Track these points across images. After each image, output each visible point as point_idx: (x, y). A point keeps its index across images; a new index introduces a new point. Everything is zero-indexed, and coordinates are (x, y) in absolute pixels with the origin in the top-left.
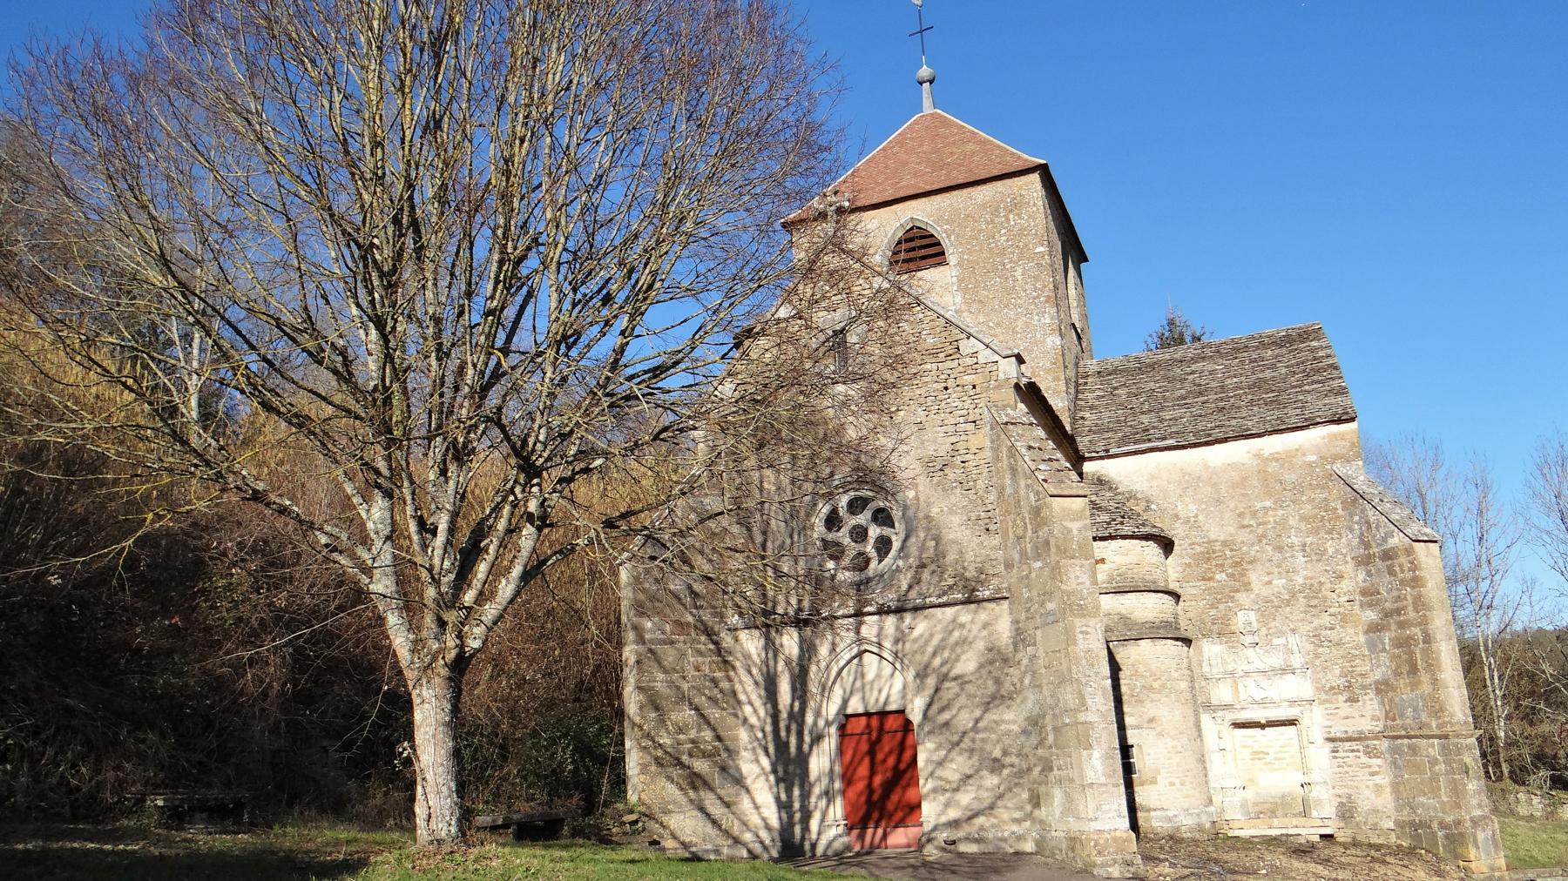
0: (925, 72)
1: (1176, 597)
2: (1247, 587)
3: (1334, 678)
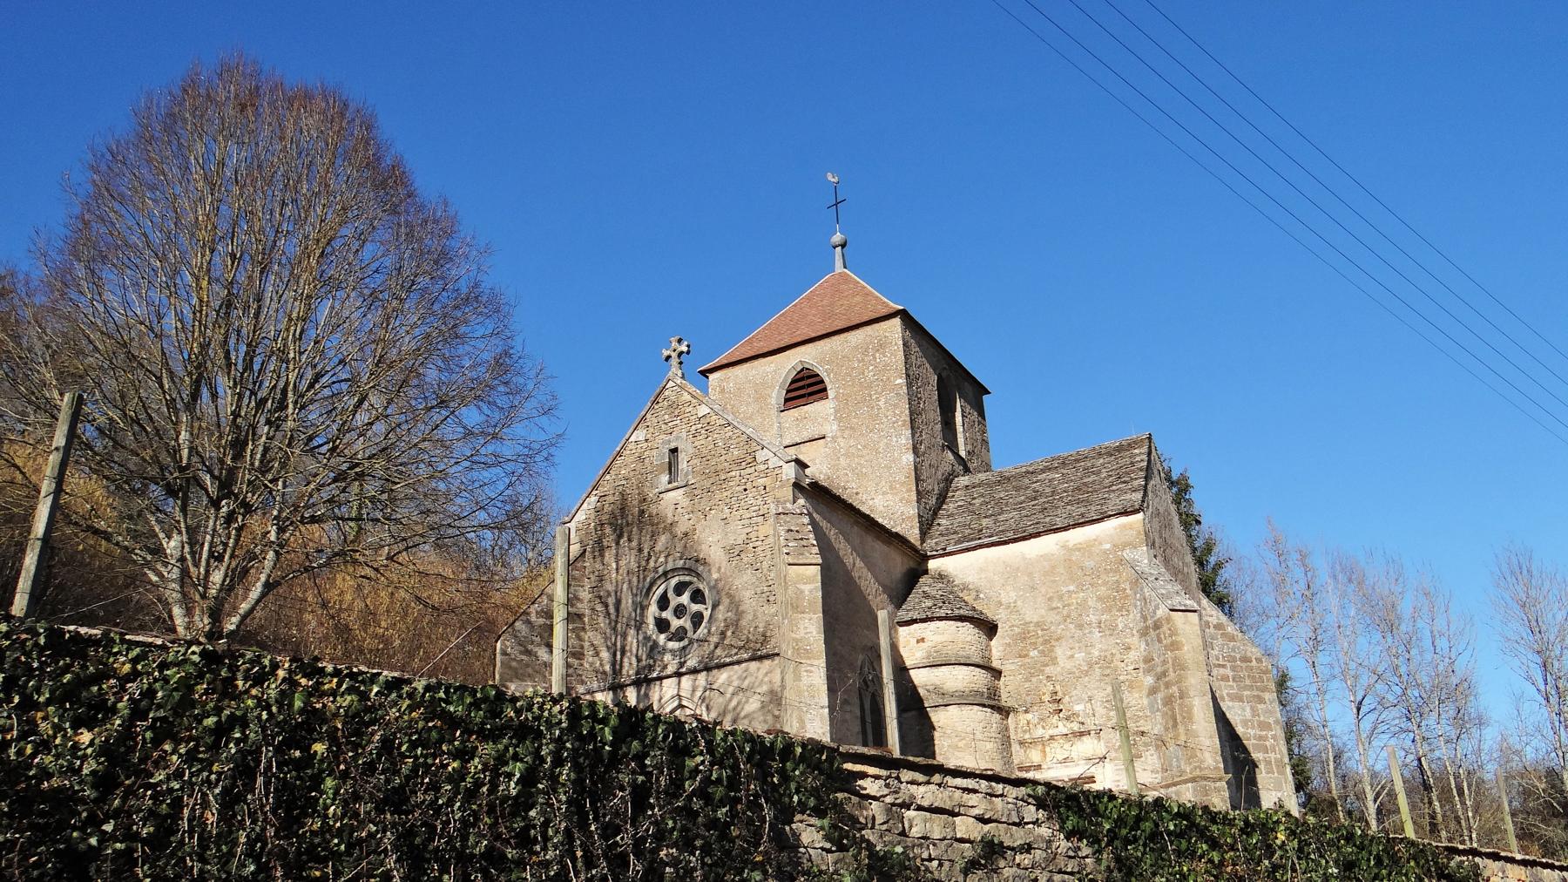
0: (837, 238)
1: (997, 674)
2: (1054, 661)
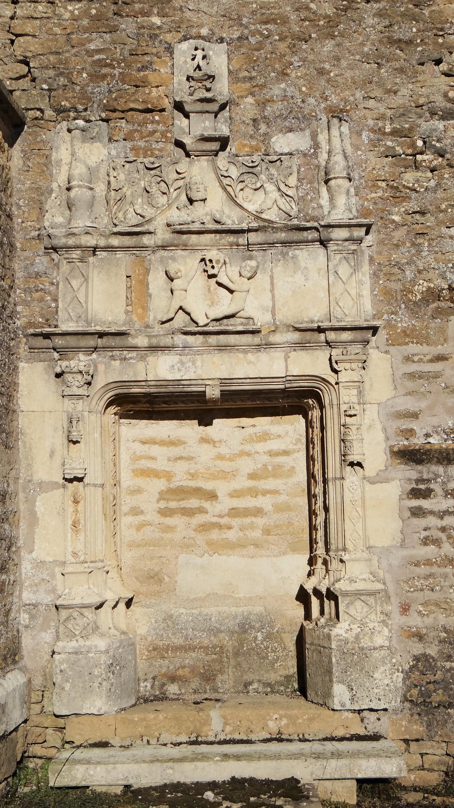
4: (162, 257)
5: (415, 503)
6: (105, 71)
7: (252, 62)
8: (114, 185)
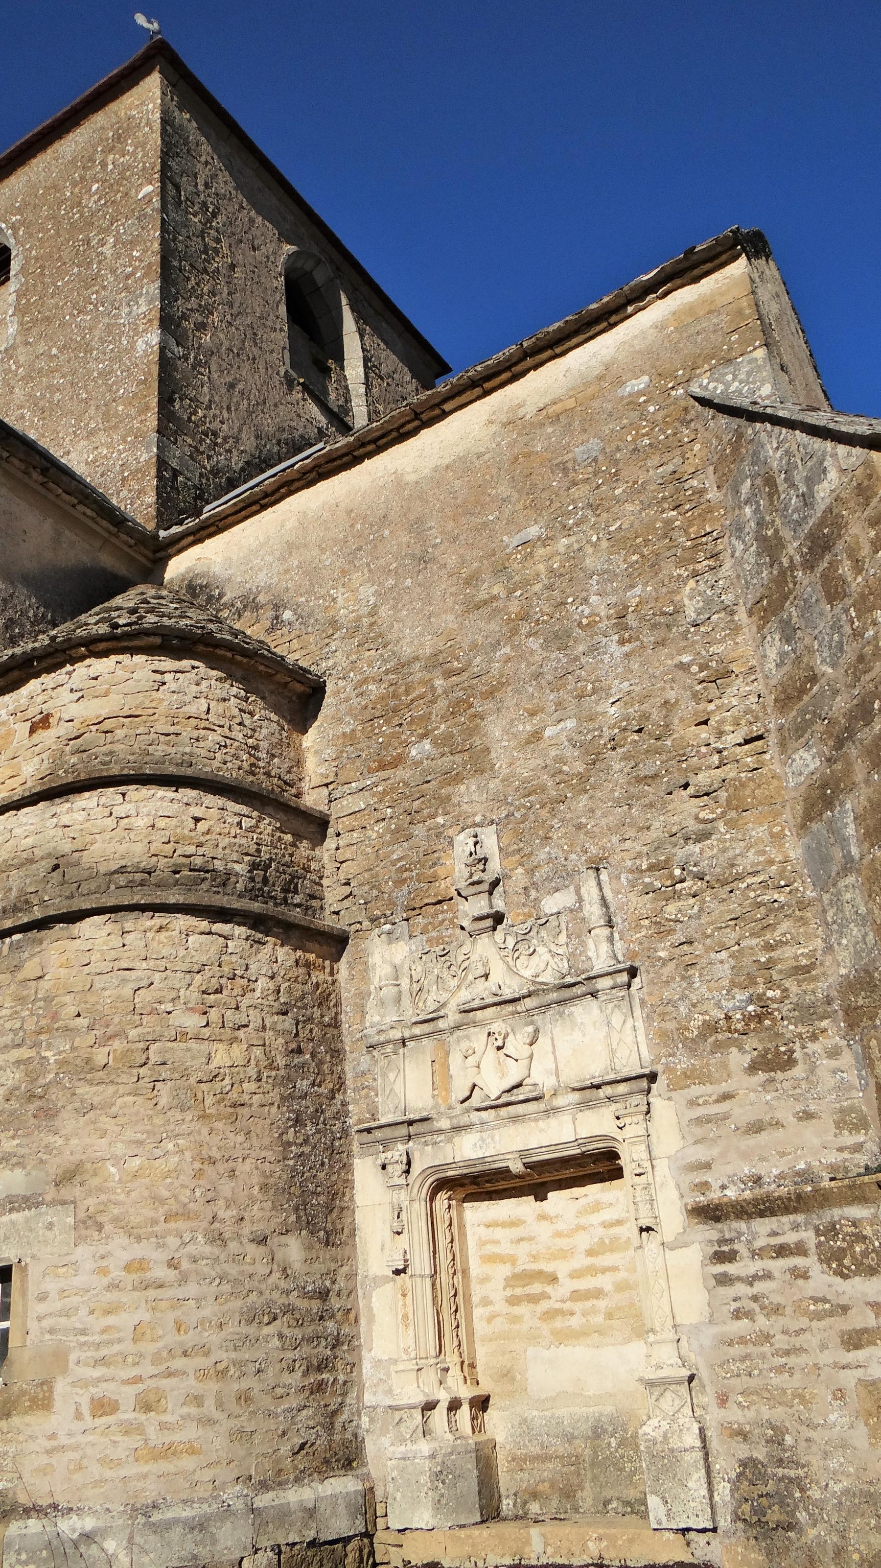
2: (479, 762)
3: (717, 994)
4: (458, 1037)
5: (720, 1268)
6: (405, 875)
7: (519, 835)
8: (415, 979)
